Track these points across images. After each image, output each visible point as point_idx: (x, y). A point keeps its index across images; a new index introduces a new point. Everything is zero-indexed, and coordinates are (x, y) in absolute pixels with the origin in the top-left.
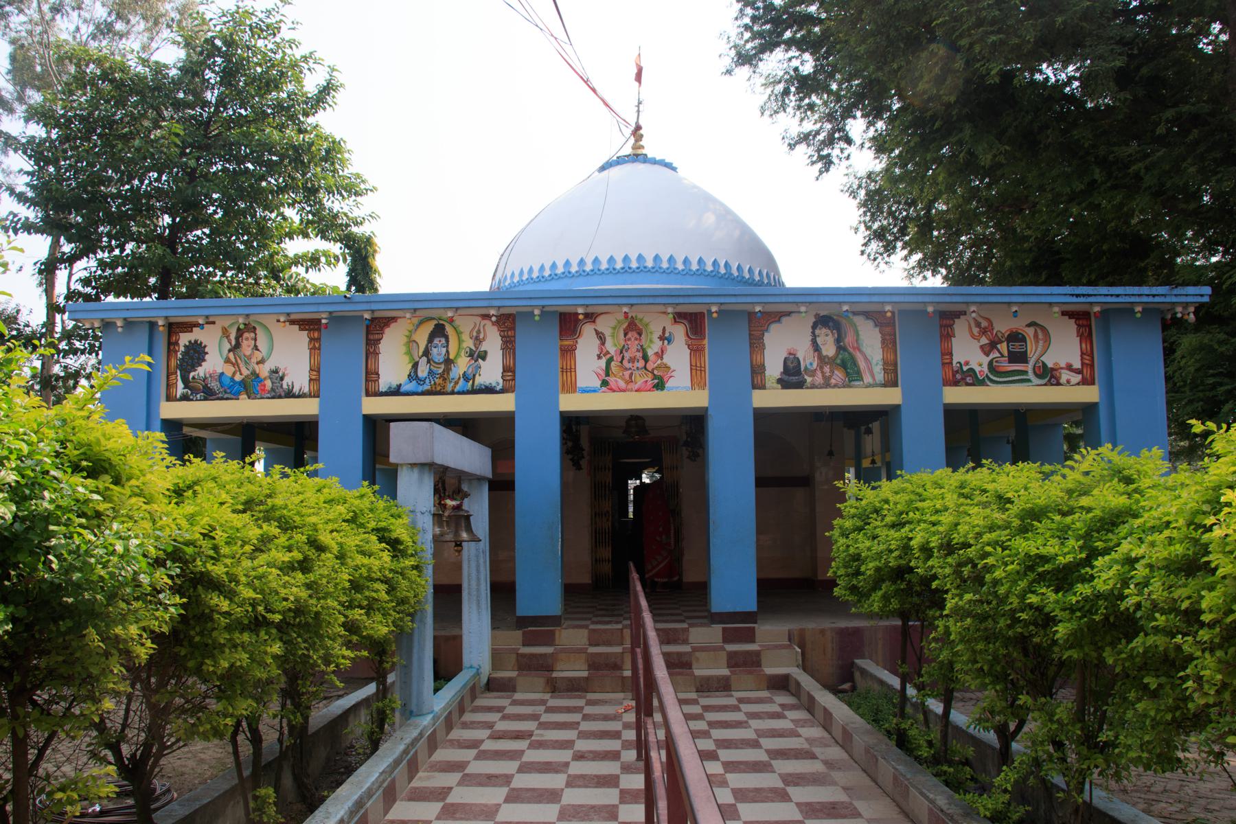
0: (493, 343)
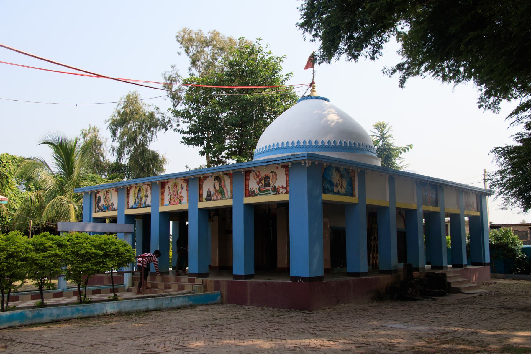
0: (149, 193)
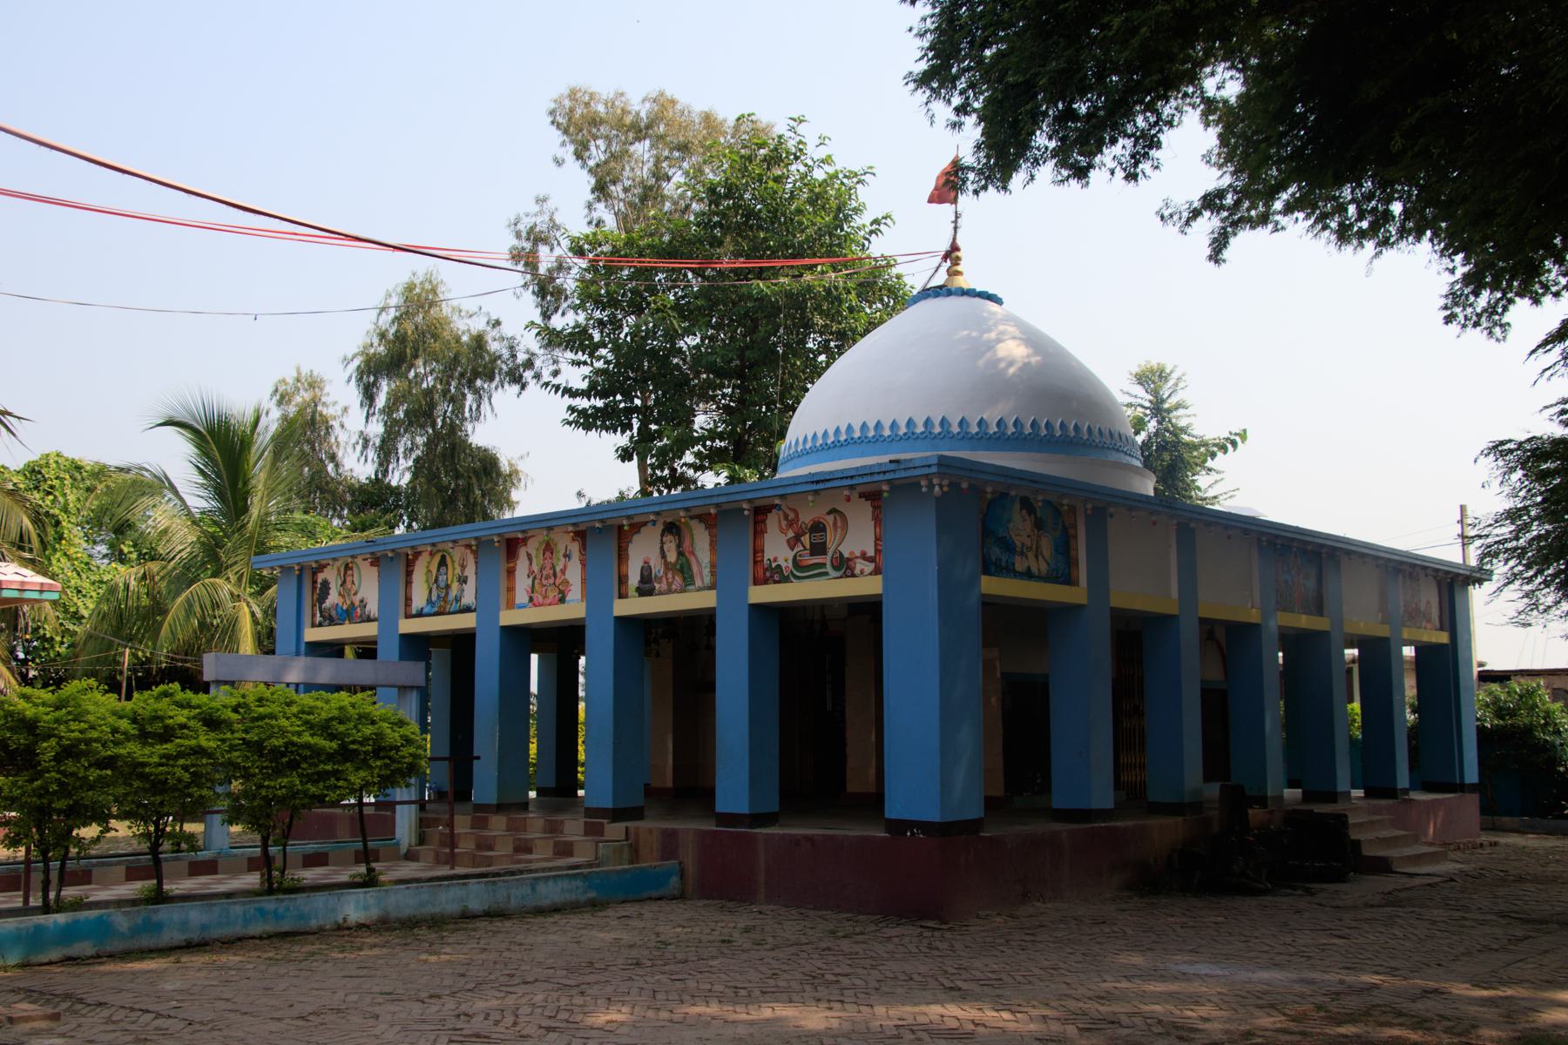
0: (470, 572)
